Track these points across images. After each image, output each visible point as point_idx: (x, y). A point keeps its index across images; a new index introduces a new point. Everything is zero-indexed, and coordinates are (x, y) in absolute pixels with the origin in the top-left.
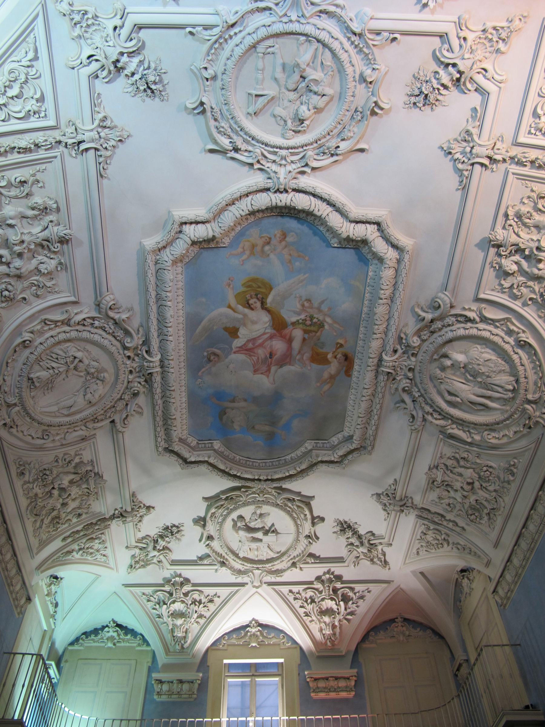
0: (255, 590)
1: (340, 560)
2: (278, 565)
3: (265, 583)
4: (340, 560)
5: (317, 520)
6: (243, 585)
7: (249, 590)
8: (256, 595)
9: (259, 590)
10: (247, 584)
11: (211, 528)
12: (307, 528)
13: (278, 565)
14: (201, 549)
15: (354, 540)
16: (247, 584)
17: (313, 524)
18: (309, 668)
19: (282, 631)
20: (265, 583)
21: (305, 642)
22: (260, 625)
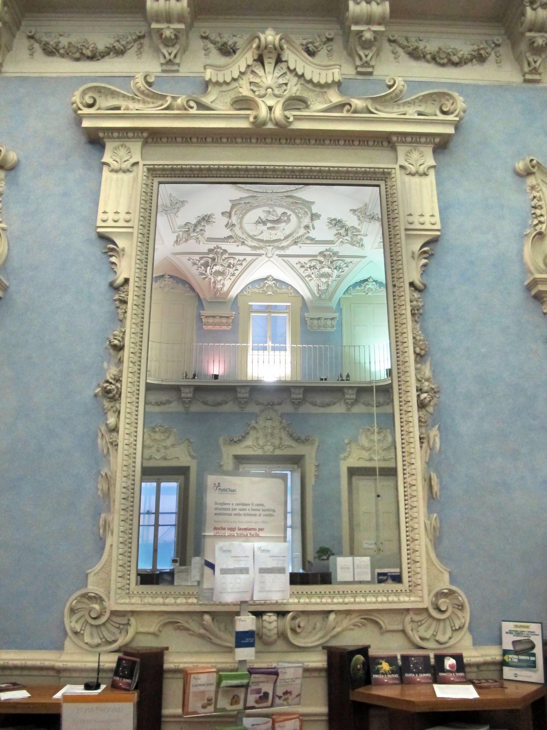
0: (267, 259)
1: (332, 242)
2: (285, 244)
3: (277, 255)
4: (332, 242)
5: (314, 217)
6: (260, 255)
7: (264, 258)
8: (269, 262)
9: (271, 259)
10: (263, 254)
11: (234, 219)
12: (306, 221)
13: (285, 244)
14: (227, 233)
15: (342, 231)
16: (263, 254)
17: (312, 219)
18: (308, 311)
19: (288, 285)
20: (277, 255)
21: (305, 293)
22: (274, 280)
